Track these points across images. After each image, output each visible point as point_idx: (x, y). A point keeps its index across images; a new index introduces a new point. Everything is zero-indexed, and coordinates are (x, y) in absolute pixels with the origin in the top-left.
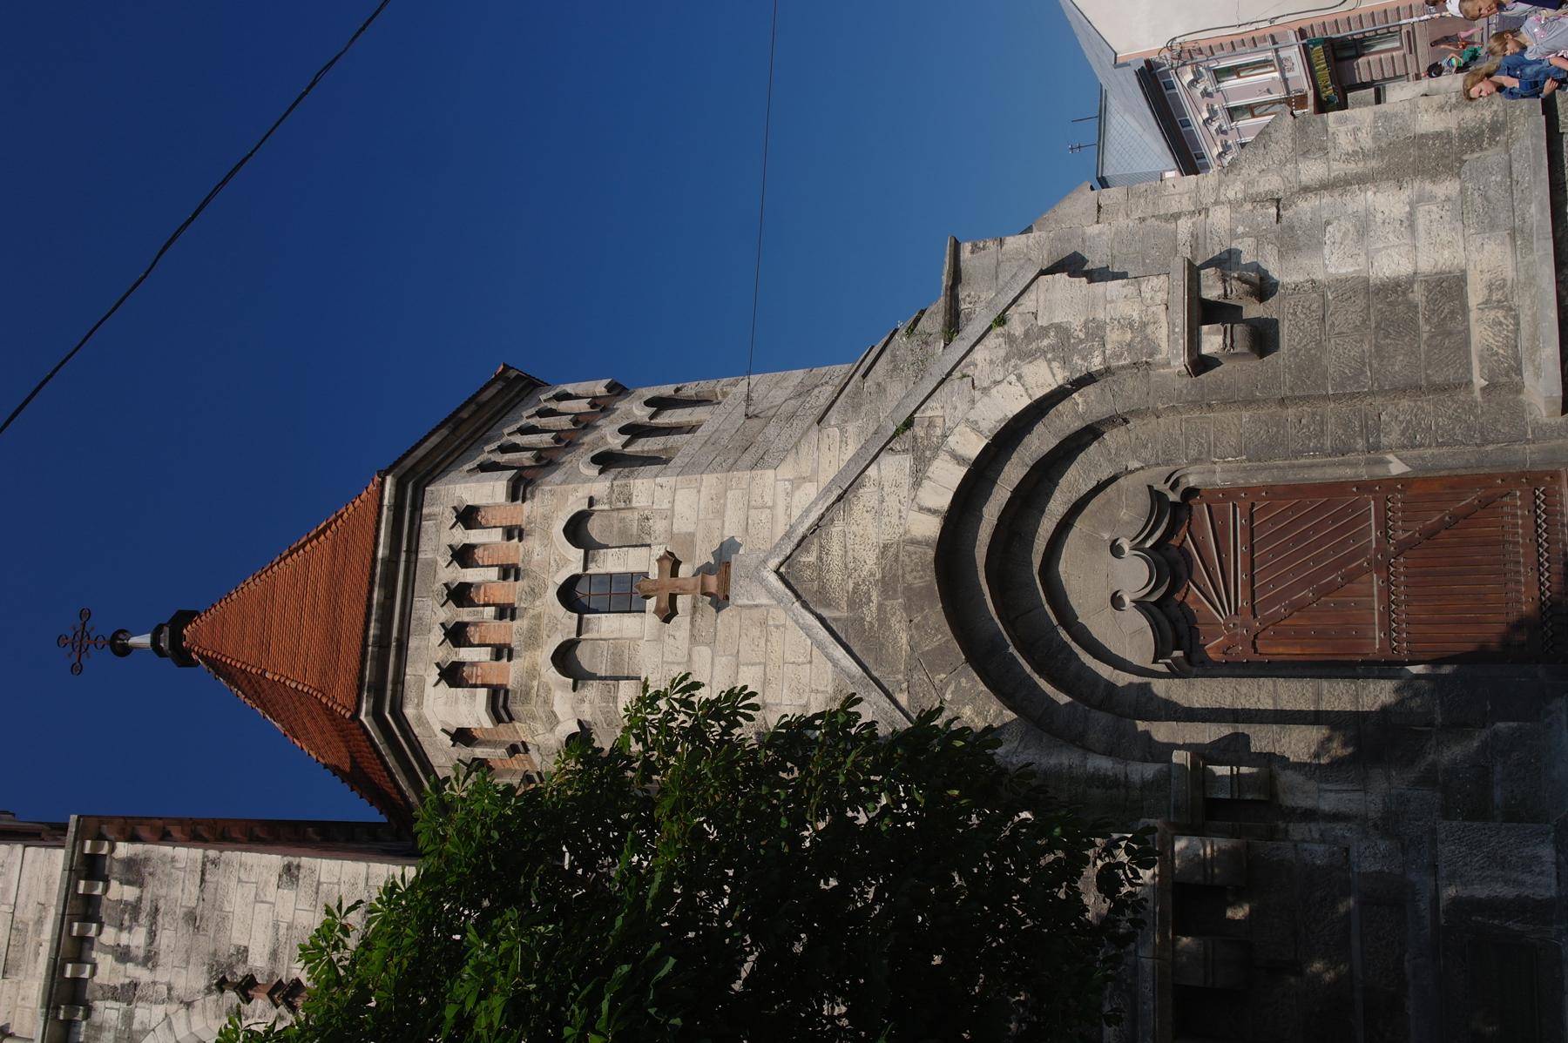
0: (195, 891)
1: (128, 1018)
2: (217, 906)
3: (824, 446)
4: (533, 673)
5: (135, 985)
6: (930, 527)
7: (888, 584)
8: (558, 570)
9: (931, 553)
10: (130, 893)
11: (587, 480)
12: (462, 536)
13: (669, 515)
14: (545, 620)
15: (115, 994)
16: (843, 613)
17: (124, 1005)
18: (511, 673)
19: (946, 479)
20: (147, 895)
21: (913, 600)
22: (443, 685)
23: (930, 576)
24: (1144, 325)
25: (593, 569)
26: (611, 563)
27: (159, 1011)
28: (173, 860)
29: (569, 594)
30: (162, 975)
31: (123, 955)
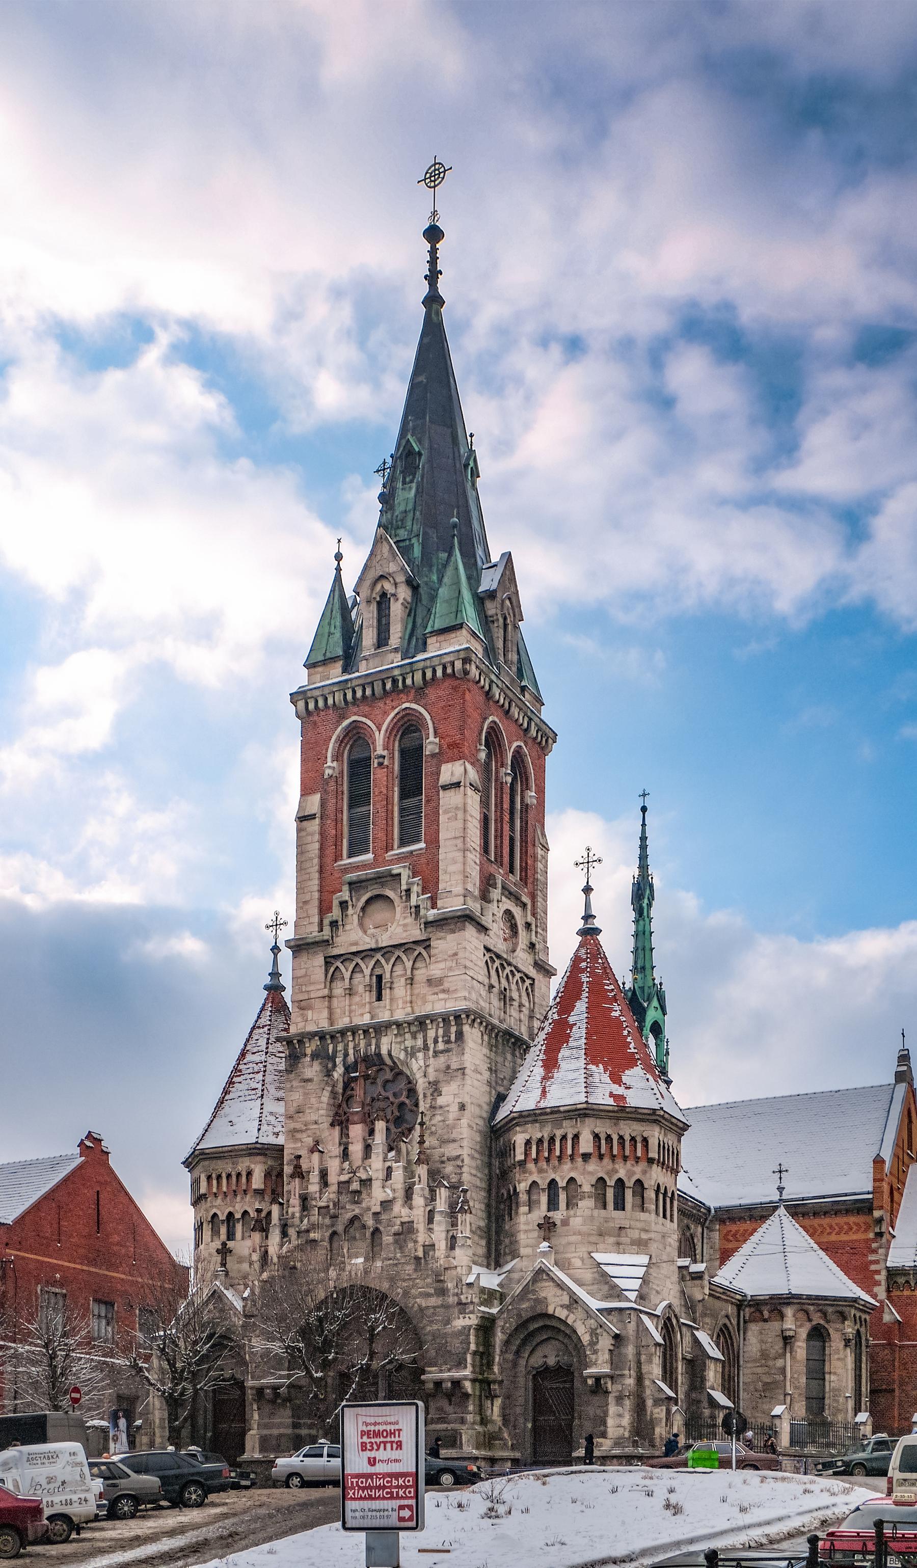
0: (455, 1067)
1: (419, 1051)
4: (531, 1173)
5: (428, 1050)
6: (550, 1311)
7: (538, 1301)
8: (561, 1176)
9: (544, 1312)
12: (570, 1137)
13: (575, 1216)
14: (545, 1174)
15: (425, 1041)
16: (531, 1288)
18: (531, 1166)
19: (562, 1313)
20: (453, 1046)
21: (532, 1308)
22: (525, 1141)
23: (539, 1312)
26: (562, 1197)
27: (421, 1063)
28: (463, 1054)
29: (553, 1183)
30: (432, 1061)
31: (436, 1041)
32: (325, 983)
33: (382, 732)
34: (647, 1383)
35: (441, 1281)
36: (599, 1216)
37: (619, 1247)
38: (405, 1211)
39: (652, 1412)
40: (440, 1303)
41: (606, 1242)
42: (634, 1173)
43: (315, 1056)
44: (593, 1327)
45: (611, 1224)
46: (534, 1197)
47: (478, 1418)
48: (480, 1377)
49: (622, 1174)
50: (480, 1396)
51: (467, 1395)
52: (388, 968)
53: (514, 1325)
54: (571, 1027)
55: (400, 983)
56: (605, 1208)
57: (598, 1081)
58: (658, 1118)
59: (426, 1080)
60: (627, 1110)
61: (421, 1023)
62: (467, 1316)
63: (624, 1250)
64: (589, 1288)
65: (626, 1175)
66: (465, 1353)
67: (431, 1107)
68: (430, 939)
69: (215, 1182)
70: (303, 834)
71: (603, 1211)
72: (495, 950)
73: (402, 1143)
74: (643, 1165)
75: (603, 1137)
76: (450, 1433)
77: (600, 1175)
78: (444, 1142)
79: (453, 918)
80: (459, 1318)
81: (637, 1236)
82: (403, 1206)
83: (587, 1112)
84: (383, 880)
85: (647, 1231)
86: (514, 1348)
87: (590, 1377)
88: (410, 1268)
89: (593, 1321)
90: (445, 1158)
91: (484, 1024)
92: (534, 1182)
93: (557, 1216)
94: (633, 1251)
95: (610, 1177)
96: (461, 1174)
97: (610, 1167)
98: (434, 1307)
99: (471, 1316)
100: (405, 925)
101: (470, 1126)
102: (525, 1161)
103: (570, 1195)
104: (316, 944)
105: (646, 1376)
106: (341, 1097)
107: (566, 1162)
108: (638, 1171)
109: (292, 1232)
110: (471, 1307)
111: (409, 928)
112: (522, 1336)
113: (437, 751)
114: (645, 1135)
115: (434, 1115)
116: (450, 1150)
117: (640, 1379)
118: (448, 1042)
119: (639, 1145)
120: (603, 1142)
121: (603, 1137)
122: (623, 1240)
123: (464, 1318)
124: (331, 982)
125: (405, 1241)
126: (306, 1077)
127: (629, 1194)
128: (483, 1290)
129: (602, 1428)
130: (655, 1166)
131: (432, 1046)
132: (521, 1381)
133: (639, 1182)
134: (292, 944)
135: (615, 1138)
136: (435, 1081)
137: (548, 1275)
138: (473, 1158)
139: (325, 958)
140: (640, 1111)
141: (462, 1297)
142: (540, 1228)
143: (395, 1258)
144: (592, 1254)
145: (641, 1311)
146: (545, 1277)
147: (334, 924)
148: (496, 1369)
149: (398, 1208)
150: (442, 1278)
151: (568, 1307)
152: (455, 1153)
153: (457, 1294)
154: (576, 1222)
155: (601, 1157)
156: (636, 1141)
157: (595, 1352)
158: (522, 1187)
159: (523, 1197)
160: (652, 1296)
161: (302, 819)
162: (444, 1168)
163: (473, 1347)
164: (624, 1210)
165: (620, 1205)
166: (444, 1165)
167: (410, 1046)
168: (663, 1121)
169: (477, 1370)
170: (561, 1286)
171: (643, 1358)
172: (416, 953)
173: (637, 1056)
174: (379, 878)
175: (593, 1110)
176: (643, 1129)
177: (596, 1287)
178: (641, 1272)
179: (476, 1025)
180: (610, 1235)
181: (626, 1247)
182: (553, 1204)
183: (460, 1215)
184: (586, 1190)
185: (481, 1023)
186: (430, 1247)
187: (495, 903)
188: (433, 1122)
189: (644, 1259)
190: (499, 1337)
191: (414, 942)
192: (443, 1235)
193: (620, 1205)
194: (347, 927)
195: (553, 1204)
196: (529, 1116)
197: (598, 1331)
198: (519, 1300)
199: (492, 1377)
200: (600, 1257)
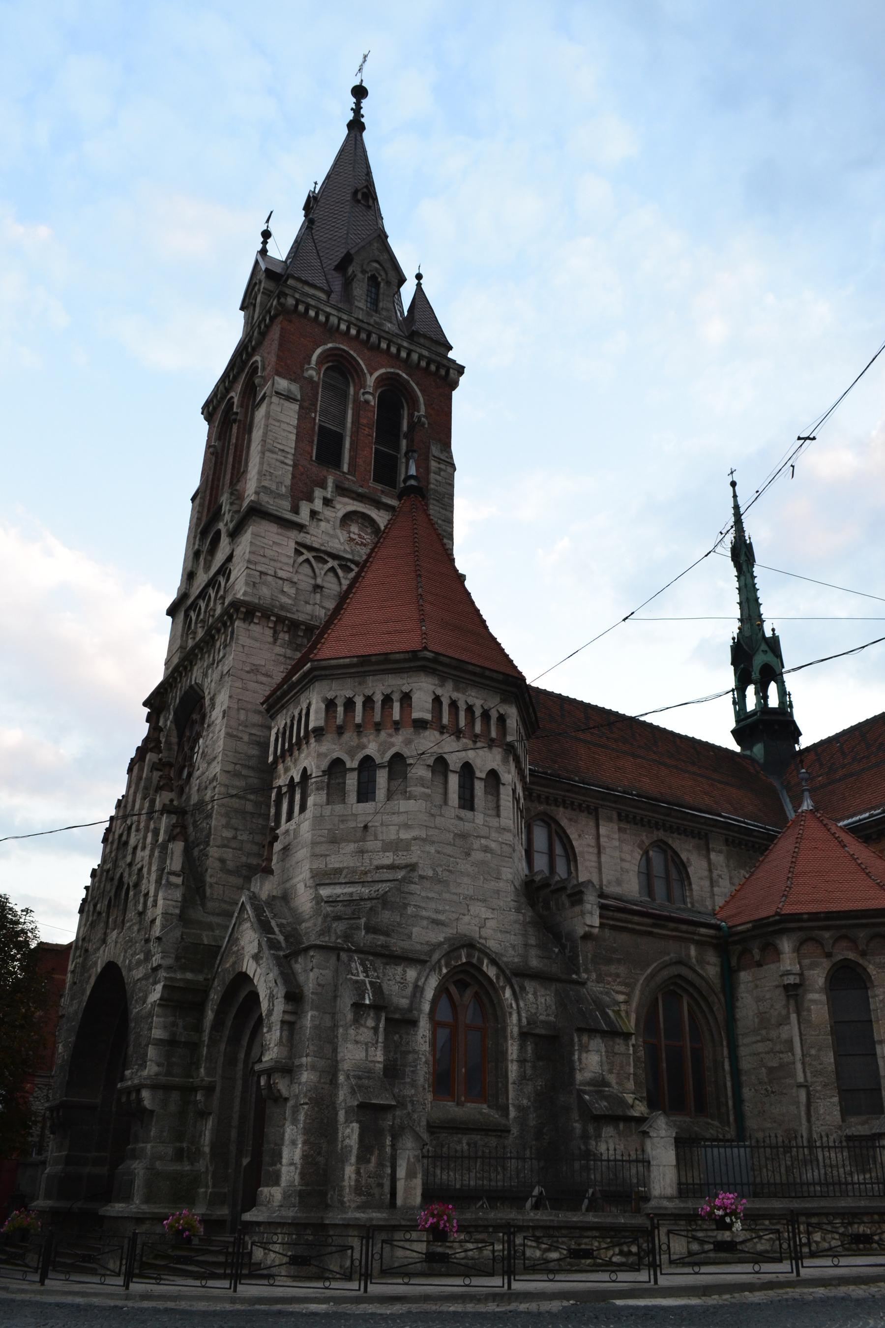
3: (311, 891)
4: (279, 777)
11: (318, 767)
12: (304, 712)
20: (228, 649)
24: (269, 1048)
36: (332, 815)
41: (342, 851)
49: (372, 749)
52: (213, 596)
56: (343, 801)
65: (379, 751)
66: (147, 1046)
71: (339, 808)
74: (407, 732)
75: (340, 702)
77: (335, 755)
81: (393, 837)
85: (407, 826)
95: (352, 760)
106: (176, 747)
107: (303, 750)
108: (398, 743)
114: (406, 689)
118: (225, 648)
119: (397, 706)
120: (340, 710)
121: (340, 702)
127: (382, 778)
131: (216, 658)
135: (359, 701)
138: (237, 775)
140: (392, 657)
149: (139, 853)
155: (340, 731)
156: (392, 700)
160: (415, 930)
164: (374, 800)
165: (366, 793)
168: (440, 668)
179: (256, 621)
180: (349, 841)
193: (366, 793)
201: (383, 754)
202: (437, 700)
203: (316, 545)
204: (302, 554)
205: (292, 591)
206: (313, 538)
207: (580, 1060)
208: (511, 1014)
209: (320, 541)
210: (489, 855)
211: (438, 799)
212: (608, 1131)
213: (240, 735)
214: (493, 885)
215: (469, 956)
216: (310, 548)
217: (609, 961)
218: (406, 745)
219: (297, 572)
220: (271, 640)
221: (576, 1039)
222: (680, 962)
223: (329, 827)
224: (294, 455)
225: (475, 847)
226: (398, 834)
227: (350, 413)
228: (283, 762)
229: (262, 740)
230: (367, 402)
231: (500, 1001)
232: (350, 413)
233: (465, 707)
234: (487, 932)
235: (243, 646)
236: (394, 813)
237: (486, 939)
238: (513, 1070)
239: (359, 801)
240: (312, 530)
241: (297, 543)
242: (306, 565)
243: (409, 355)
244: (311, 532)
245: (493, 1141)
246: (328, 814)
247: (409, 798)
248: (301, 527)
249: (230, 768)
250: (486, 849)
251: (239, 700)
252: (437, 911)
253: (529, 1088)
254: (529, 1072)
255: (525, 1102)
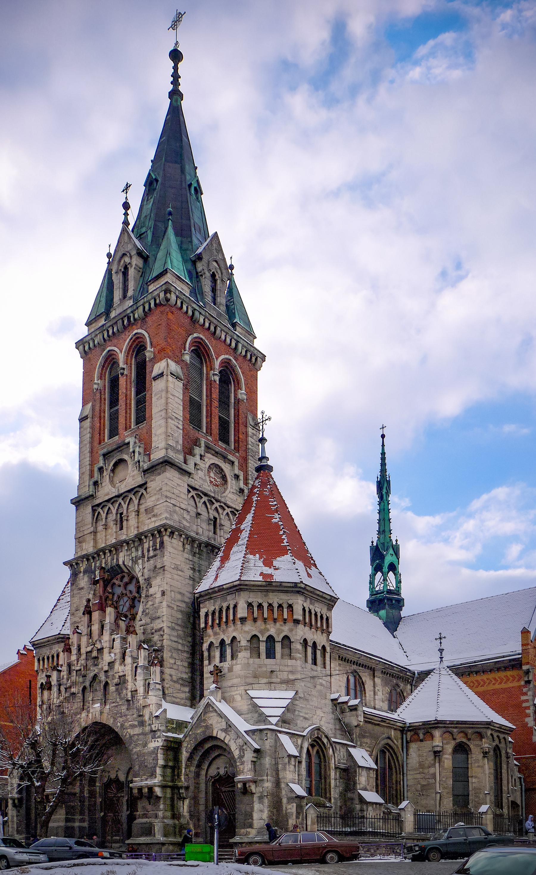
2: (157, 574)
3: (248, 700)
4: (210, 636)
5: (144, 557)
7: (207, 727)
10: (158, 547)
13: (236, 664)
14: (218, 636)
15: (143, 551)
17: (141, 555)
18: (209, 631)
20: (158, 552)
21: (204, 732)
25: (227, 646)
27: (141, 567)
28: (164, 556)
29: (222, 642)
32: (92, 523)
33: (123, 353)
34: (283, 785)
35: (140, 716)
37: (271, 686)
38: (121, 668)
39: (286, 808)
40: (141, 731)
42: (283, 631)
43: (85, 572)
44: (241, 745)
45: (264, 669)
46: (212, 654)
47: (169, 814)
48: (170, 784)
49: (272, 631)
50: (172, 799)
51: (158, 798)
53: (193, 745)
54: (241, 531)
55: (132, 515)
57: (252, 565)
58: (299, 589)
59: (143, 578)
60: (274, 584)
61: (139, 538)
62: (156, 740)
63: (275, 687)
64: (246, 716)
65: (276, 633)
67: (146, 596)
68: (146, 483)
69: (41, 662)
70: (82, 429)
71: (257, 660)
72: (200, 489)
73: (120, 621)
74: (290, 625)
76: (147, 825)
77: (254, 633)
78: (153, 619)
79: (158, 464)
80: (152, 742)
82: (121, 664)
83: (242, 587)
84: (121, 448)
85: (292, 672)
86: (195, 762)
87: (239, 782)
88: (124, 708)
89: (240, 740)
90: (154, 631)
91: (183, 536)
92: (211, 644)
93: (225, 666)
94: (282, 688)
96: (163, 640)
97: (263, 627)
98: (138, 735)
99: (159, 739)
100: (133, 476)
101: (169, 606)
102: (206, 627)
103: (234, 649)
104: (87, 498)
105: (282, 781)
108: (286, 629)
109: (62, 688)
110: (158, 734)
111: (136, 477)
112: (200, 754)
113: (152, 356)
114: (290, 602)
115: (148, 602)
116: (157, 625)
117: (277, 783)
118: (155, 550)
119: (285, 610)
122: (274, 680)
123: (155, 741)
124: (96, 523)
125: (122, 689)
126: (81, 587)
127: (278, 647)
128: (171, 721)
129: (250, 820)
130: (301, 626)
132: (203, 786)
133: (286, 637)
134: (74, 501)
136: (148, 578)
137: (213, 707)
139: (93, 507)
141: (153, 726)
142: (212, 675)
143: (116, 702)
144: (248, 692)
145: (280, 732)
146: (211, 710)
147: (96, 483)
148: (183, 778)
150: (141, 714)
151: (225, 731)
152: (159, 626)
153: (150, 725)
154: (237, 668)
155: (255, 620)
157: (243, 763)
158: (205, 646)
159: (206, 654)
160: (298, 722)
161: (82, 420)
162: (153, 637)
163: (161, 762)
165: (270, 654)
166: (153, 636)
167: (134, 556)
168: (306, 592)
169: (169, 779)
170: (221, 715)
171: (280, 766)
172: (140, 494)
173: (288, 548)
174: (120, 447)
175: (246, 585)
176: (287, 598)
177: (250, 715)
178: (285, 703)
179: (175, 537)
181: (277, 685)
182: (223, 658)
183: (152, 667)
184: (244, 645)
185: (181, 536)
186: (135, 692)
187: (198, 457)
188: (147, 606)
189: (291, 694)
190: (184, 755)
191: (140, 486)
192: (142, 683)
193: (270, 654)
194: (103, 485)
195: (223, 658)
196: (206, 595)
197: (244, 747)
198: (196, 727)
199: (180, 784)
200: (252, 693)
201: (278, 635)
202: (304, 610)
203: (197, 487)
204: (190, 492)
205: (188, 517)
206: (196, 482)
207: (359, 779)
208: (332, 759)
209: (199, 484)
210: (322, 687)
211: (304, 658)
212: (370, 808)
213: (173, 606)
214: (323, 701)
215: (318, 734)
216: (194, 489)
217: (364, 737)
218: (290, 631)
219: (188, 504)
220: (182, 549)
221: (358, 771)
222: (389, 738)
223: (253, 670)
224: (183, 422)
225: (318, 683)
226: (288, 676)
227: (205, 387)
228: (212, 629)
229: (182, 609)
230: (215, 381)
231: (328, 753)
232: (205, 387)
233: (308, 610)
234: (322, 723)
235: (170, 552)
236: (285, 666)
237: (322, 726)
238: (333, 782)
239: (266, 658)
240: (195, 477)
241: (188, 485)
242: (192, 499)
243: (236, 345)
244: (194, 478)
245: (326, 810)
246: (252, 663)
247: (293, 659)
248: (189, 474)
249: (170, 625)
250: (321, 685)
251: (171, 585)
252: (306, 714)
253: (338, 791)
254: (338, 783)
255: (337, 796)
